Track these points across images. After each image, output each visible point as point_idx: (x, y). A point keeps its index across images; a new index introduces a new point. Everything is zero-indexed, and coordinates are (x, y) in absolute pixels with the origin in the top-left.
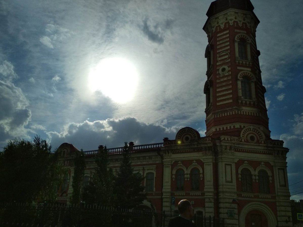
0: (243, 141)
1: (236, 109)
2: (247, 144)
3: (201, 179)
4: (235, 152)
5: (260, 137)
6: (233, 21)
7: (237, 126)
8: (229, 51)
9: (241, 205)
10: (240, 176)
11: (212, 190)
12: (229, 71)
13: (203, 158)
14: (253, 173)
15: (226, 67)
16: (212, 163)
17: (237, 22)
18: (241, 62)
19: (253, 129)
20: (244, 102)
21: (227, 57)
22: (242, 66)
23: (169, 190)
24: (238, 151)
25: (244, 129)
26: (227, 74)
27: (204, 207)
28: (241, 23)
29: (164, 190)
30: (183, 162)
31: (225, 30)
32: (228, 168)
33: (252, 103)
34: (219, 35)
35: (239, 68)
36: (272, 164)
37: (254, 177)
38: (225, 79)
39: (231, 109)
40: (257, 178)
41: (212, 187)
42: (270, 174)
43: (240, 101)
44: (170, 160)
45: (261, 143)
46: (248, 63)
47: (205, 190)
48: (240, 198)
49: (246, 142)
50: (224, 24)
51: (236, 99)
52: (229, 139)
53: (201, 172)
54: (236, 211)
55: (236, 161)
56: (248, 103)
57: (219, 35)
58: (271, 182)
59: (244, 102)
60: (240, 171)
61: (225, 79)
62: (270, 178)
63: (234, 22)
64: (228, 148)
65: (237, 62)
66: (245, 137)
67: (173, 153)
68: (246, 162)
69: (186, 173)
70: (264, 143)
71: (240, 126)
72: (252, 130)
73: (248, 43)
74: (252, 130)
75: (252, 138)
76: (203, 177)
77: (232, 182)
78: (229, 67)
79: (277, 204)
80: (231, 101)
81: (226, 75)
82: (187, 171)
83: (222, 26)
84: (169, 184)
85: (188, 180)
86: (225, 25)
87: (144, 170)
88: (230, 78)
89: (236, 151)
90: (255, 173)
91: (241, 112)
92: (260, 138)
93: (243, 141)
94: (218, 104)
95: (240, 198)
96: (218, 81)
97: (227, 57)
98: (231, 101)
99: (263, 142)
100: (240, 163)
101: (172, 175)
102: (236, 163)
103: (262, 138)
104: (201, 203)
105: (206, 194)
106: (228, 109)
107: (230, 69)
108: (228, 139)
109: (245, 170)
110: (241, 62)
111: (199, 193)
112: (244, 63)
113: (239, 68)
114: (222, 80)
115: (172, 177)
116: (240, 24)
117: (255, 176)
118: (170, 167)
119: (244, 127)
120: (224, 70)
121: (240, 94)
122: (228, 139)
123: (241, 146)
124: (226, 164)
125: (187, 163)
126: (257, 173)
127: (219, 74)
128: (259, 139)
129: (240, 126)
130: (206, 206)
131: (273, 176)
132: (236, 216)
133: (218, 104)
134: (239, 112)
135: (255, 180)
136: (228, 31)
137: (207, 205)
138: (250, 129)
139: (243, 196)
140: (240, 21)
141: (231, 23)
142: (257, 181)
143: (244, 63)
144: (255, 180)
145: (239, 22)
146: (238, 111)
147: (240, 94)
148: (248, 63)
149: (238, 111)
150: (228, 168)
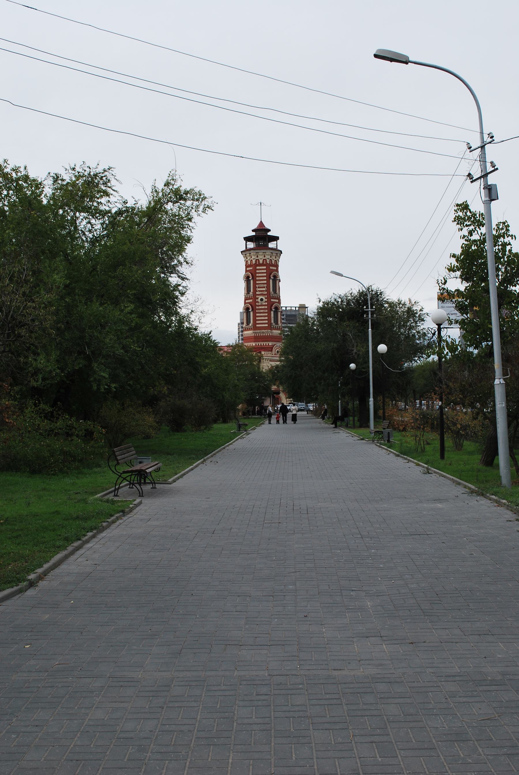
12: (266, 302)
26: (264, 304)
31: (262, 265)
38: (263, 307)
61: (263, 307)
78: (266, 298)
88: (266, 307)
94: (257, 326)
96: (257, 308)
106: (264, 331)
107: (266, 300)
114: (260, 307)
120: (262, 300)
121: (272, 321)
127: (258, 302)
133: (257, 326)
136: (265, 267)
147: (272, 321)
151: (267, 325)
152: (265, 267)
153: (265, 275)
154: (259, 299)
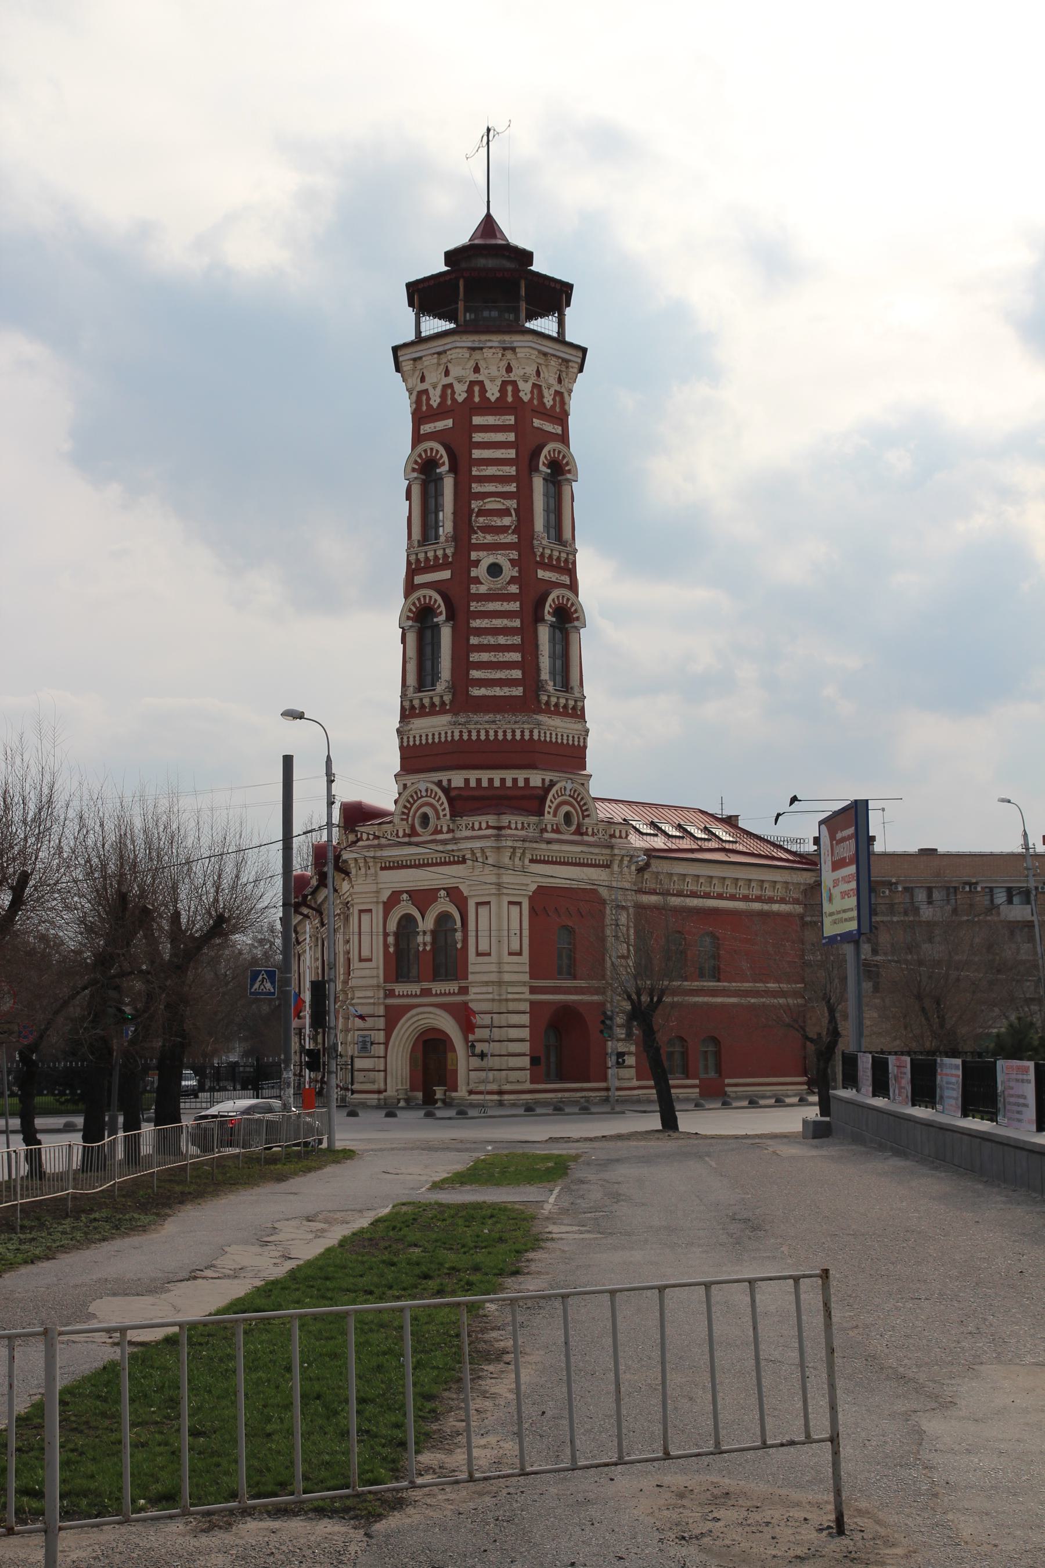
0: (401, 834)
9: (393, 1016)
10: (391, 940)
18: (421, 556)
20: (416, 703)
37: (420, 939)
43: (407, 704)
45: (441, 832)
48: (390, 1001)
49: (409, 836)
54: (381, 1036)
55: (385, 896)
59: (416, 703)
60: (392, 926)
74: (424, 794)
75: (425, 819)
89: (382, 869)
93: (401, 834)
95: (390, 1001)
99: (445, 829)
102: (384, 903)
112: (431, 554)
117: (425, 933)
132: (380, 1050)
134: (405, 740)
135: (425, 944)
142: (428, 948)
143: (431, 554)
144: (425, 944)
148: (440, 553)
151: (518, 691)
152: (511, 420)
153: (511, 454)
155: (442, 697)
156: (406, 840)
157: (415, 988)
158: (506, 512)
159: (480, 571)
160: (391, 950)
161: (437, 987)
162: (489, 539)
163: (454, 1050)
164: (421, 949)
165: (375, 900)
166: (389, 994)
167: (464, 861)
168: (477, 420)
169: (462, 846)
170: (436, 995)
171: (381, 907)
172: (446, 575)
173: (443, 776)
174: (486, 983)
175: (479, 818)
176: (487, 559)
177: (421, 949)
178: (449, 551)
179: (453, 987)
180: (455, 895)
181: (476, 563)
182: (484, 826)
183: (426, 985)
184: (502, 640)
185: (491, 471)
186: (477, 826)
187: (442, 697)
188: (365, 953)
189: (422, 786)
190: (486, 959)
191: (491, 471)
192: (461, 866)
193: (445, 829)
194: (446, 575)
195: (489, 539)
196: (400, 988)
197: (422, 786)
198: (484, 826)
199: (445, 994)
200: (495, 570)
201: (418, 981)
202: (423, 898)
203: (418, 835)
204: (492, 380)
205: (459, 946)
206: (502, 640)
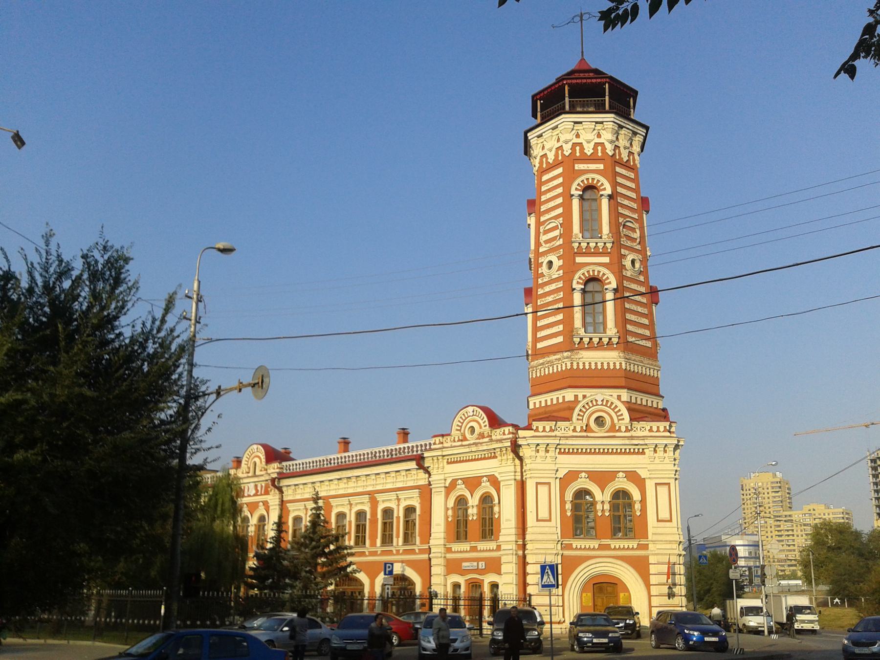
0: (578, 429)
1: (567, 358)
2: (589, 434)
3: (497, 516)
4: (559, 456)
5: (618, 416)
6: (570, 145)
7: (569, 395)
8: (561, 220)
10: (568, 506)
11: (513, 538)
12: (560, 268)
13: (500, 470)
14: (598, 495)
15: (553, 258)
16: (513, 482)
17: (580, 144)
18: (584, 245)
19: (602, 401)
21: (556, 233)
22: (588, 253)
23: (442, 542)
24: (564, 453)
25: (586, 400)
27: (499, 573)
28: (592, 145)
29: (432, 542)
30: (466, 481)
32: (543, 490)
33: (605, 340)
34: (545, 178)
35: (579, 260)
36: (643, 474)
37: (599, 507)
39: (559, 359)
40: (607, 507)
41: (513, 531)
42: (636, 495)
44: (442, 477)
45: (619, 430)
46: (600, 245)
47: (501, 538)
50: (554, 150)
51: (569, 332)
52: (548, 429)
53: (496, 501)
55: (561, 474)
56: (596, 340)
57: (545, 178)
58: (638, 513)
60: (569, 496)
62: (637, 506)
63: (574, 145)
64: (542, 448)
65: (576, 245)
66: (585, 421)
67: (448, 463)
68: (583, 475)
69: (470, 504)
70: (627, 430)
71: (576, 396)
72: (600, 403)
73: (602, 195)
74: (600, 403)
76: (499, 513)
77: (550, 520)
78: (559, 258)
79: (652, 559)
80: (560, 339)
81: (554, 277)
82: (473, 501)
83: (551, 157)
84: (442, 528)
85: (475, 518)
86: (556, 155)
87: (398, 500)
89: (560, 453)
90: (602, 497)
91: (578, 363)
92: (619, 420)
93: (578, 429)
94: (540, 345)
95: (567, 553)
97: (556, 233)
98: (560, 339)
99: (623, 429)
100: (572, 476)
101: (447, 509)
103: (623, 419)
104: (494, 566)
105: (502, 548)
108: (544, 427)
109: (581, 494)
110: (584, 245)
111: (492, 545)
112: (592, 245)
113: (579, 260)
115: (446, 513)
116: (589, 150)
118: (443, 493)
119: (584, 397)
122: (544, 427)
123: (570, 442)
124: (537, 484)
125: (472, 483)
126: (607, 497)
127: (542, 275)
128: (616, 421)
129: (576, 396)
130: (503, 571)
131: (643, 501)
133: (540, 345)
135: (603, 510)
136: (560, 170)
137: (504, 568)
138: (596, 401)
139: (574, 547)
140: (589, 142)
141: (567, 151)
142: (607, 514)
143: (592, 245)
145: (585, 144)
146: (572, 363)
148: (600, 245)
149: (572, 363)
150: (543, 490)
151: (649, 344)
154: (545, 265)
155: (610, 339)
156: (584, 434)
157: (595, 544)
158: (633, 230)
159: (627, 263)
160: (569, 514)
161: (614, 543)
162: (629, 244)
163: (627, 590)
164: (600, 514)
165: (554, 475)
166: (569, 547)
167: (643, 453)
168: (618, 169)
169: (647, 442)
170: (615, 549)
171: (558, 480)
172: (606, 260)
173: (615, 392)
174: (671, 542)
175: (658, 424)
176: (630, 258)
177: (600, 514)
178: (609, 245)
179: (633, 544)
180: (632, 476)
181: (624, 256)
182: (662, 429)
183: (605, 542)
184: (640, 309)
185: (626, 202)
186: (655, 429)
187: (610, 339)
188: (543, 514)
189: (599, 398)
190: (668, 524)
191: (626, 202)
192: (640, 456)
193: (623, 429)
194: (606, 260)
195: (629, 244)
196: (576, 543)
197: (599, 398)
198: (662, 429)
199: (624, 548)
200: (633, 262)
201: (596, 537)
202: (602, 478)
203: (593, 432)
204: (625, 148)
205: (638, 513)
206: (640, 309)
